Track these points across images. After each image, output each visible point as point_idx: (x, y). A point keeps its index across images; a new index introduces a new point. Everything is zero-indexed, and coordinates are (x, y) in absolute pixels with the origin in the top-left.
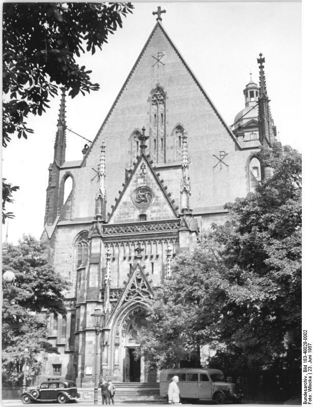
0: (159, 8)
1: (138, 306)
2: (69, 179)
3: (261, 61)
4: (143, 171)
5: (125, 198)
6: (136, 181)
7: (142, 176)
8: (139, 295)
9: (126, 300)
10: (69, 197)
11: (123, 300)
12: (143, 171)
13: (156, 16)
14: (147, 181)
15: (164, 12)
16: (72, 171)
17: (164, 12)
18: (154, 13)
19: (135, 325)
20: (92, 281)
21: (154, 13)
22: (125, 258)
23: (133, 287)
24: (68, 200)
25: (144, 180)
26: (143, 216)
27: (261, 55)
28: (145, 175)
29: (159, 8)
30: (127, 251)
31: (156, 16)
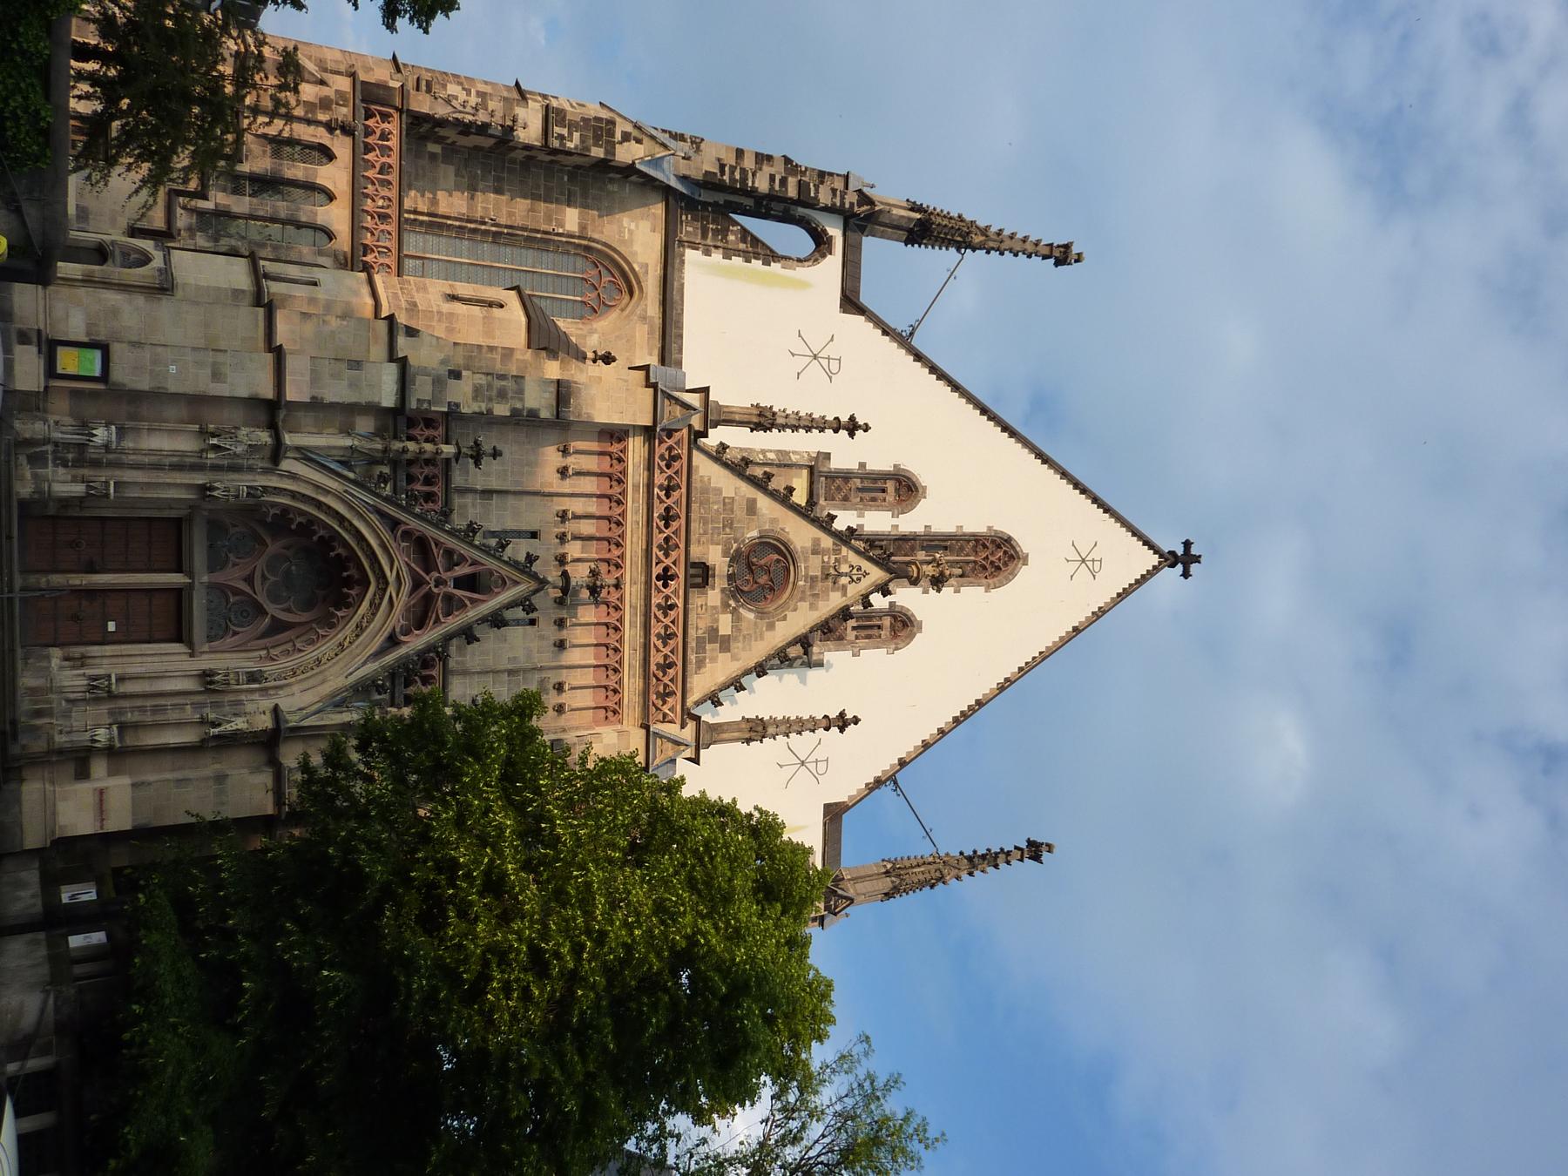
0: (1197, 559)
1: (372, 579)
2: (808, 245)
3: (1035, 851)
4: (846, 575)
5: (764, 503)
6: (816, 551)
7: (831, 576)
8: (418, 583)
9: (403, 527)
10: (756, 241)
11: (402, 516)
12: (846, 575)
13: (1180, 551)
14: (812, 587)
15: (1186, 574)
16: (832, 264)
17: (1186, 574)
18: (1187, 544)
19: (287, 548)
20: (490, 386)
21: (1187, 544)
22: (563, 516)
23: (452, 559)
24: (745, 233)
25: (813, 579)
26: (701, 575)
27: (1050, 848)
28: (830, 584)
29: (1197, 559)
30: (587, 528)
31: (1180, 551)
